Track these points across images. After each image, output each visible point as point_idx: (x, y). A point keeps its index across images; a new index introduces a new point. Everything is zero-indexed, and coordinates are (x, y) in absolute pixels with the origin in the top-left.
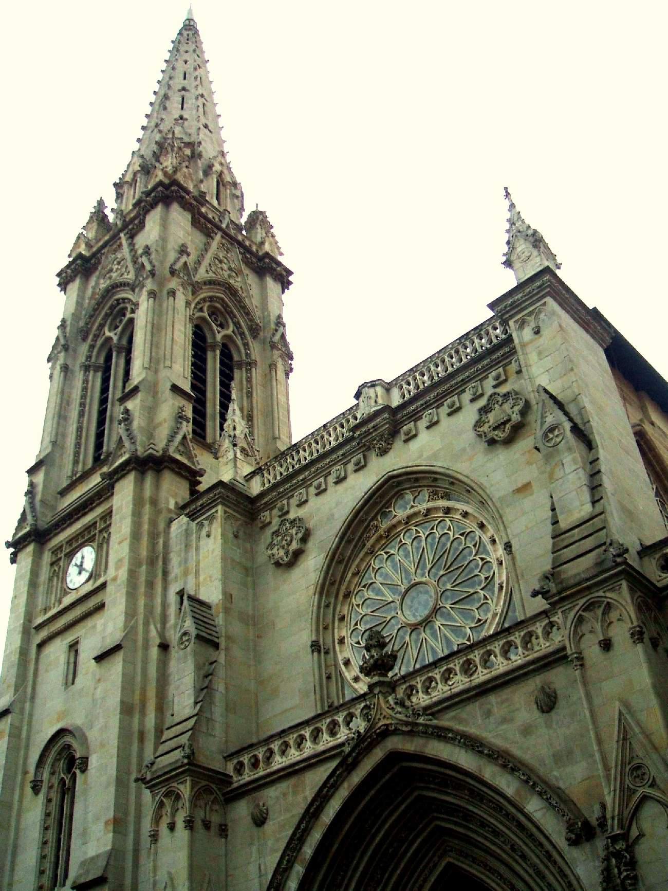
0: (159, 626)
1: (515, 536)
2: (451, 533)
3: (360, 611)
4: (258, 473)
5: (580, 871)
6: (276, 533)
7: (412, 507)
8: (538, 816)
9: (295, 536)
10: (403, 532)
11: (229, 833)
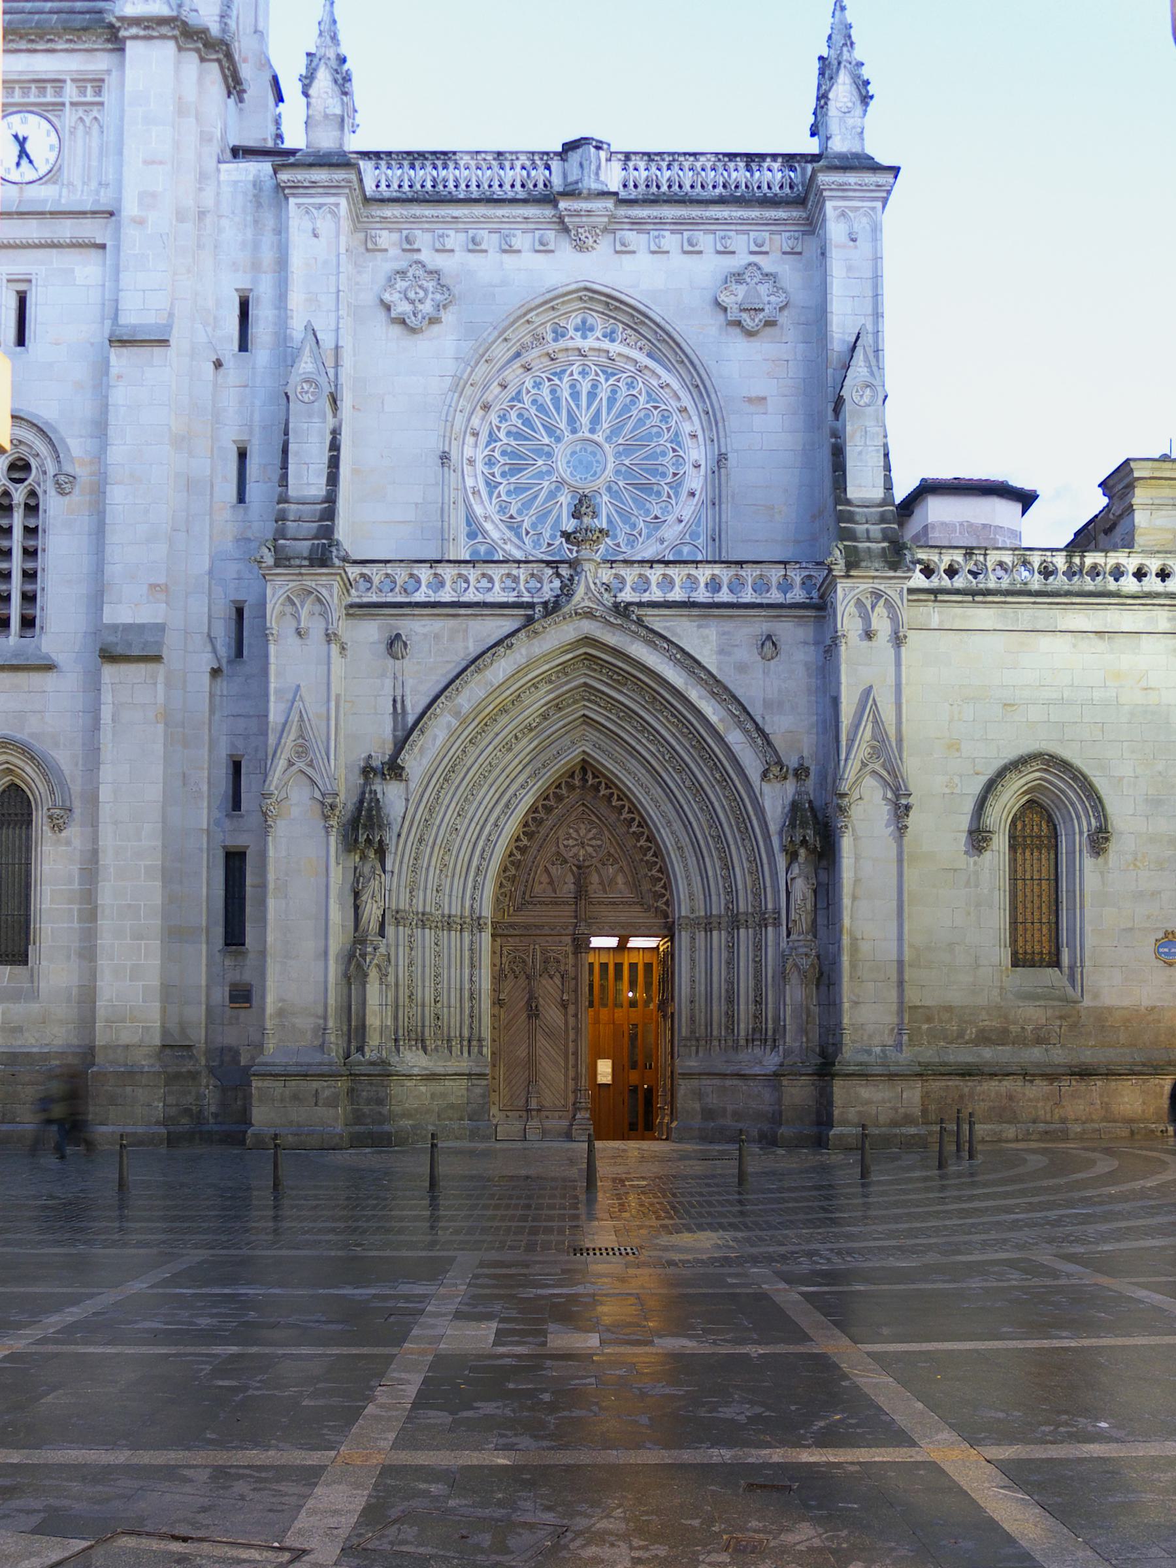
0: (209, 329)
1: (737, 451)
2: (642, 399)
3: (502, 435)
4: (370, 159)
5: (767, 804)
6: (402, 273)
7: (598, 339)
8: (736, 748)
9: (430, 296)
10: (578, 363)
11: (348, 653)
